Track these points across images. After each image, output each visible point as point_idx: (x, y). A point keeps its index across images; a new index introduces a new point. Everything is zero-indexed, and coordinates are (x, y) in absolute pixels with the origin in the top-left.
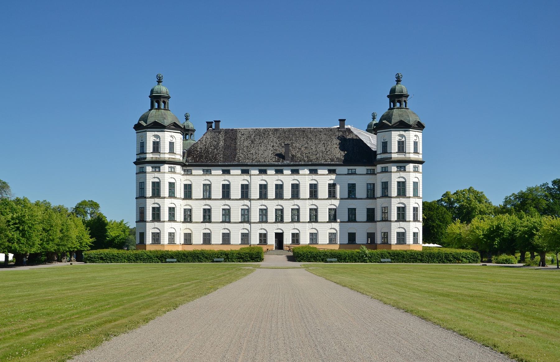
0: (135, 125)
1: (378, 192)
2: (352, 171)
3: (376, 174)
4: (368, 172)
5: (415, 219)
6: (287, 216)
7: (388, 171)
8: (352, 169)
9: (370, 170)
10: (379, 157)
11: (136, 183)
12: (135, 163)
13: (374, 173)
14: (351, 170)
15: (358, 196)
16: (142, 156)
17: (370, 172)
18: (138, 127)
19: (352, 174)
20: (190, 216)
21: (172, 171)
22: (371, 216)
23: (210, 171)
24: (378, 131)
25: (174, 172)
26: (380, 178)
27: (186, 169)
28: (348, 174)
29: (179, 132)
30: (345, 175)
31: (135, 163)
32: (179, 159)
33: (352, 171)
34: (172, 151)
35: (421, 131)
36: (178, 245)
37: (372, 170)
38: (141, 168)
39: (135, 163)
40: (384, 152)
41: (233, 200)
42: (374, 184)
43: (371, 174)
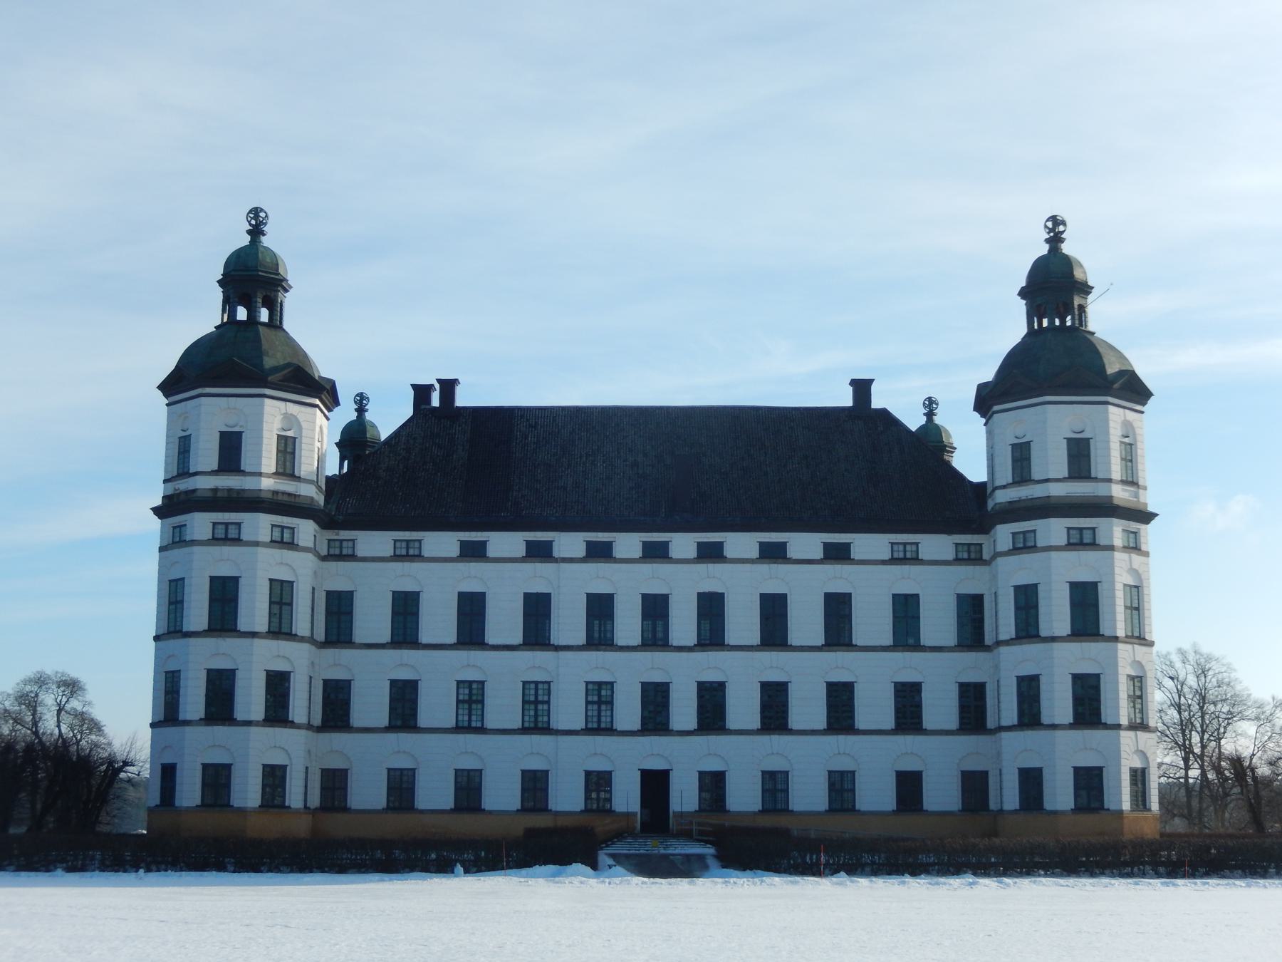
2: (905, 551)
4: (960, 556)
6: (684, 711)
7: (1035, 546)
8: (905, 544)
9: (966, 548)
10: (1002, 497)
11: (160, 581)
12: (159, 512)
13: (981, 559)
14: (901, 548)
15: (927, 638)
17: (965, 555)
18: (173, 386)
19: (903, 561)
20: (346, 705)
21: (285, 542)
23: (417, 545)
24: (996, 408)
25: (292, 545)
27: (336, 537)
28: (893, 561)
29: (317, 402)
30: (883, 562)
31: (159, 512)
32: (312, 498)
33: (905, 551)
35: (1138, 407)
36: (297, 811)
37: (972, 548)
38: (178, 529)
39: (157, 511)
40: (1016, 480)
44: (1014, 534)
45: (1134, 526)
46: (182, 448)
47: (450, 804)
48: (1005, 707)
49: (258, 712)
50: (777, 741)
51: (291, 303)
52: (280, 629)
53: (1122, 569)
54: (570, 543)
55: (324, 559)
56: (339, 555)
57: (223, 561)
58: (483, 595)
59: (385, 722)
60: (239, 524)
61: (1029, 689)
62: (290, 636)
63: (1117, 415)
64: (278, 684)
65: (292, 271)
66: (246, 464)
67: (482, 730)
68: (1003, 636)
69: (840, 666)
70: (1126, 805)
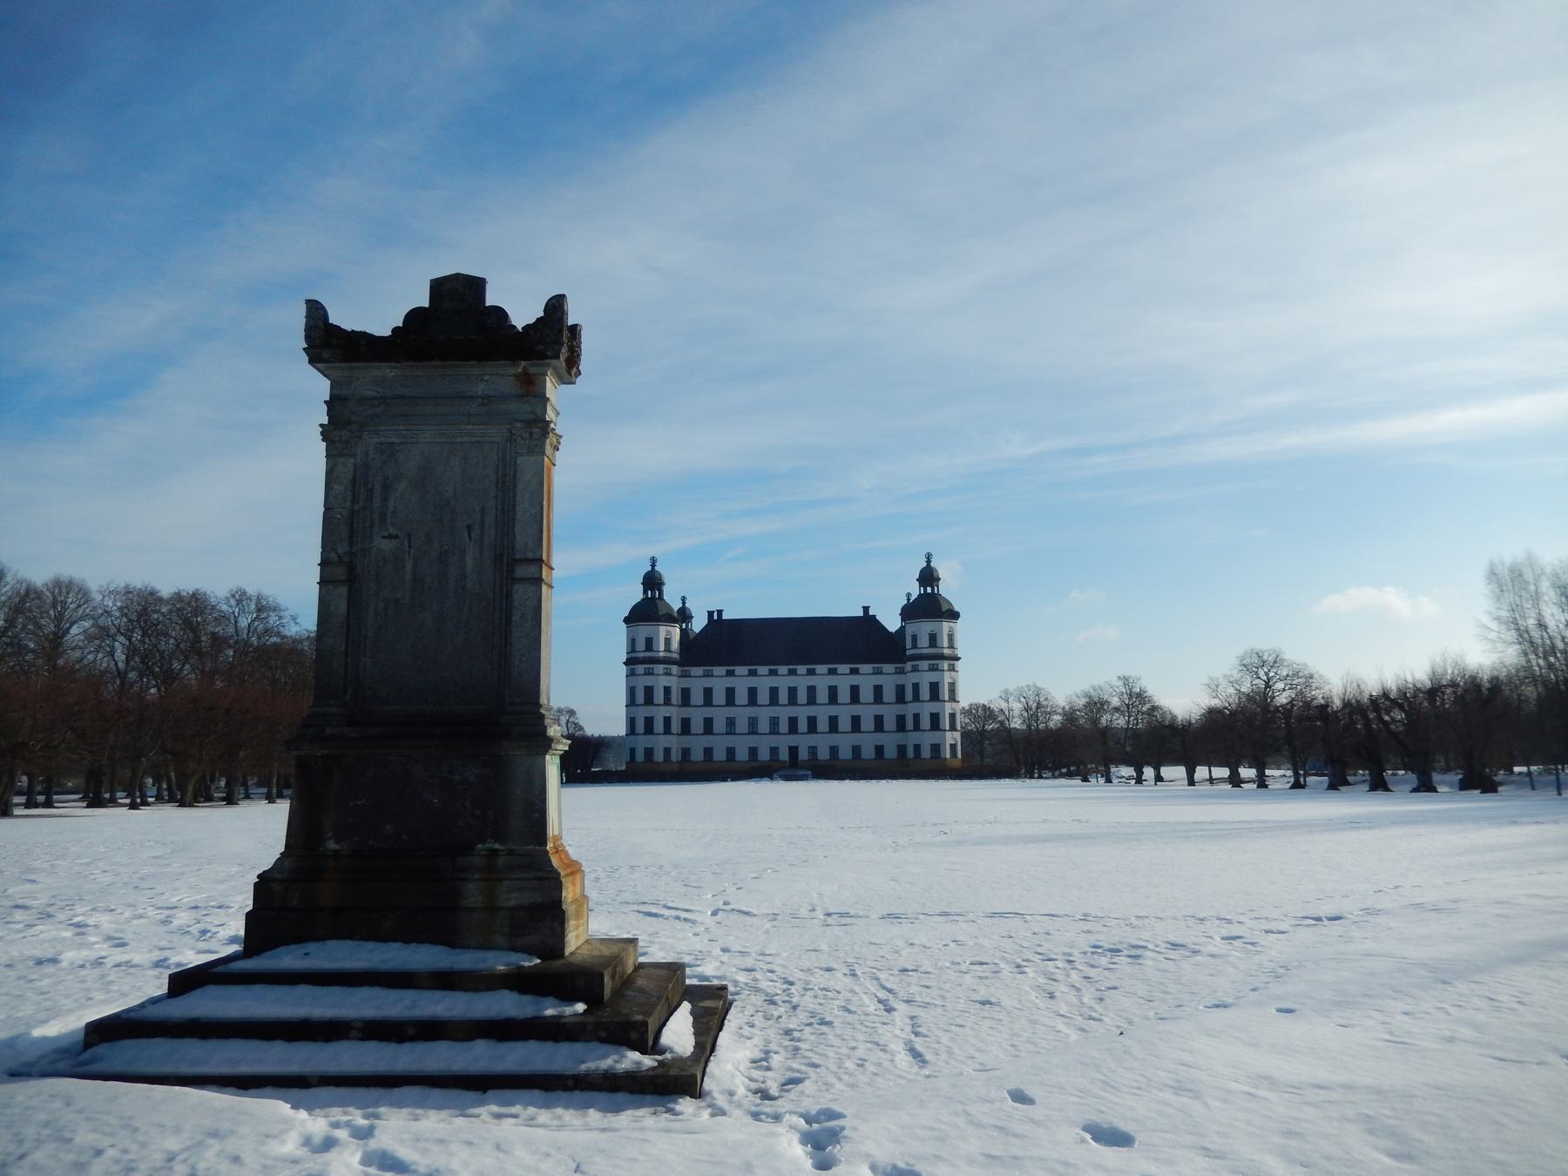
0: (626, 618)
1: (909, 695)
3: (905, 674)
5: (953, 728)
10: (908, 653)
16: (634, 655)
18: (627, 620)
21: (668, 674)
22: (901, 722)
25: (670, 674)
26: (909, 680)
28: (874, 673)
34: (668, 649)
41: (738, 706)
42: (904, 686)
43: (900, 673)
44: (912, 666)
45: (953, 662)
46: (632, 643)
47: (725, 759)
48: (910, 724)
49: (662, 731)
50: (834, 736)
51: (665, 589)
52: (667, 701)
53: (947, 678)
54: (763, 670)
55: (680, 677)
56: (685, 675)
57: (648, 681)
58: (734, 688)
59: (702, 732)
60: (653, 669)
61: (917, 717)
62: (671, 705)
63: (946, 626)
64: (667, 720)
65: (666, 579)
66: (655, 648)
67: (735, 734)
68: (909, 700)
69: (856, 710)
70: (948, 756)
